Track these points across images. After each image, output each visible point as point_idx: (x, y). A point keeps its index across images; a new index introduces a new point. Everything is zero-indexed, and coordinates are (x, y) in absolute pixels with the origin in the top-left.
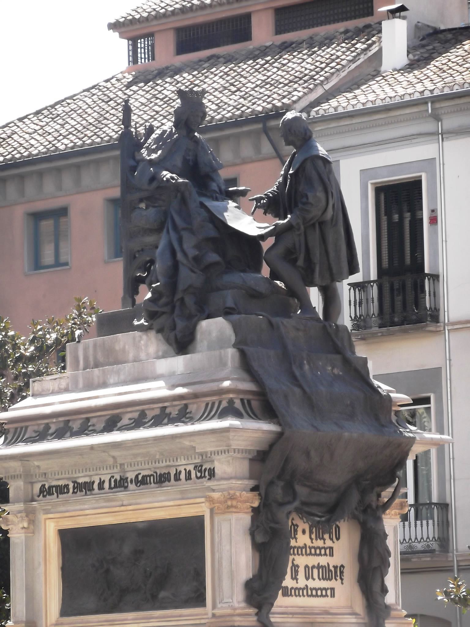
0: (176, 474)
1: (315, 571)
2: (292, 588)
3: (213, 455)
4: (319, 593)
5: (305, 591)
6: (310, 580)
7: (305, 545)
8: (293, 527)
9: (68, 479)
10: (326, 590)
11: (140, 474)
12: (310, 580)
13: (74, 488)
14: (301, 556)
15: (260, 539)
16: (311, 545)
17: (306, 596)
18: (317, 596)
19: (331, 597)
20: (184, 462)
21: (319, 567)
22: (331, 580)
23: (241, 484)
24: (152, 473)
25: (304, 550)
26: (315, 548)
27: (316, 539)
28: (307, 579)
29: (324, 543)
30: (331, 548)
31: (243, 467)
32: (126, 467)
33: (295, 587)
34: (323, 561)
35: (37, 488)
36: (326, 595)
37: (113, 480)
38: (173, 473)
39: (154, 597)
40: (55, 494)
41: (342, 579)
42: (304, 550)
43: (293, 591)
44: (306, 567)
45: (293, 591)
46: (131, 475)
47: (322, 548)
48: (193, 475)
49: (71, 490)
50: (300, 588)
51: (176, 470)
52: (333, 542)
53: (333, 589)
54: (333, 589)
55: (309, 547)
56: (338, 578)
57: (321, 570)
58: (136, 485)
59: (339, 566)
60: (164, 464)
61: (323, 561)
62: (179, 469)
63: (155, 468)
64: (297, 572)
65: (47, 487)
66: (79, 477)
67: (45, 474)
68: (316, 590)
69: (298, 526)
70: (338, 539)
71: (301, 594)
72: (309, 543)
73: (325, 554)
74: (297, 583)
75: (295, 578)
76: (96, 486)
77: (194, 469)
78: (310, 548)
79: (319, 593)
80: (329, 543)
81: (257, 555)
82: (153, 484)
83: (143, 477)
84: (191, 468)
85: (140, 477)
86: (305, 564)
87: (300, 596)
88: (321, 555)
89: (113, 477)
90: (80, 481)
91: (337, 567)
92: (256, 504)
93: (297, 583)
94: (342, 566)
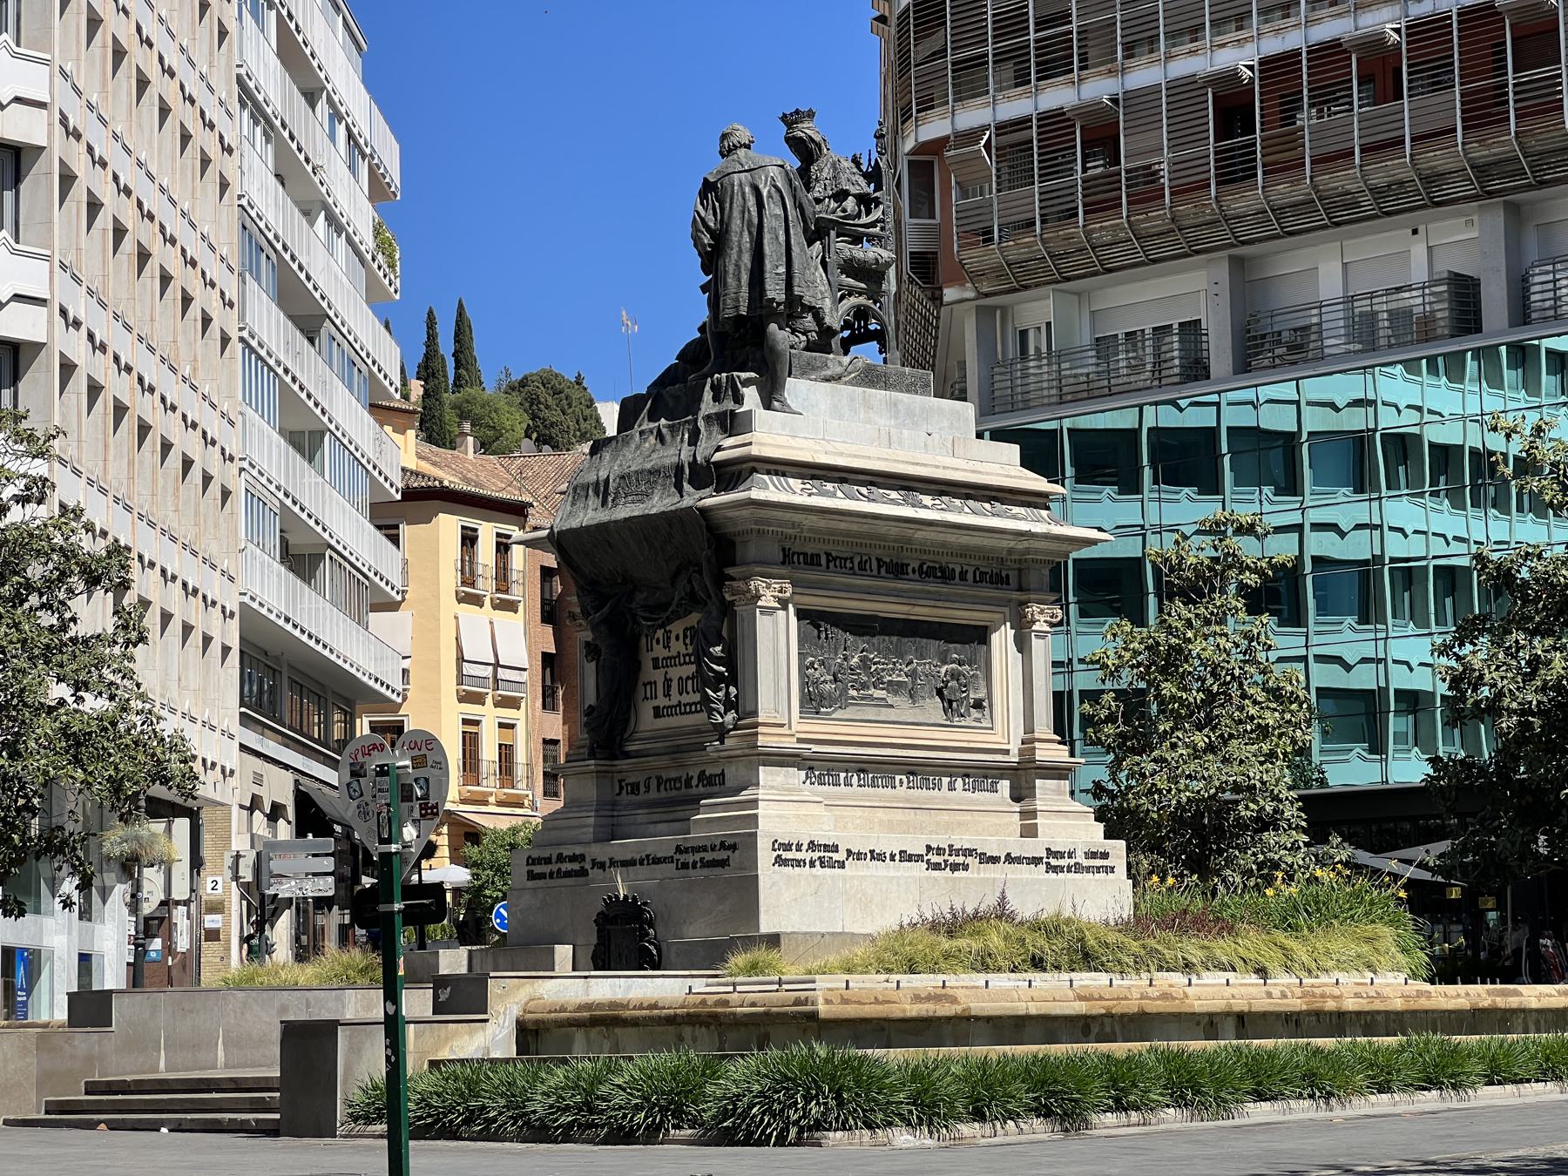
18: (691, 712)
28: (681, 694)
64: (669, 686)
68: (691, 705)
75: (667, 695)
78: (684, 656)
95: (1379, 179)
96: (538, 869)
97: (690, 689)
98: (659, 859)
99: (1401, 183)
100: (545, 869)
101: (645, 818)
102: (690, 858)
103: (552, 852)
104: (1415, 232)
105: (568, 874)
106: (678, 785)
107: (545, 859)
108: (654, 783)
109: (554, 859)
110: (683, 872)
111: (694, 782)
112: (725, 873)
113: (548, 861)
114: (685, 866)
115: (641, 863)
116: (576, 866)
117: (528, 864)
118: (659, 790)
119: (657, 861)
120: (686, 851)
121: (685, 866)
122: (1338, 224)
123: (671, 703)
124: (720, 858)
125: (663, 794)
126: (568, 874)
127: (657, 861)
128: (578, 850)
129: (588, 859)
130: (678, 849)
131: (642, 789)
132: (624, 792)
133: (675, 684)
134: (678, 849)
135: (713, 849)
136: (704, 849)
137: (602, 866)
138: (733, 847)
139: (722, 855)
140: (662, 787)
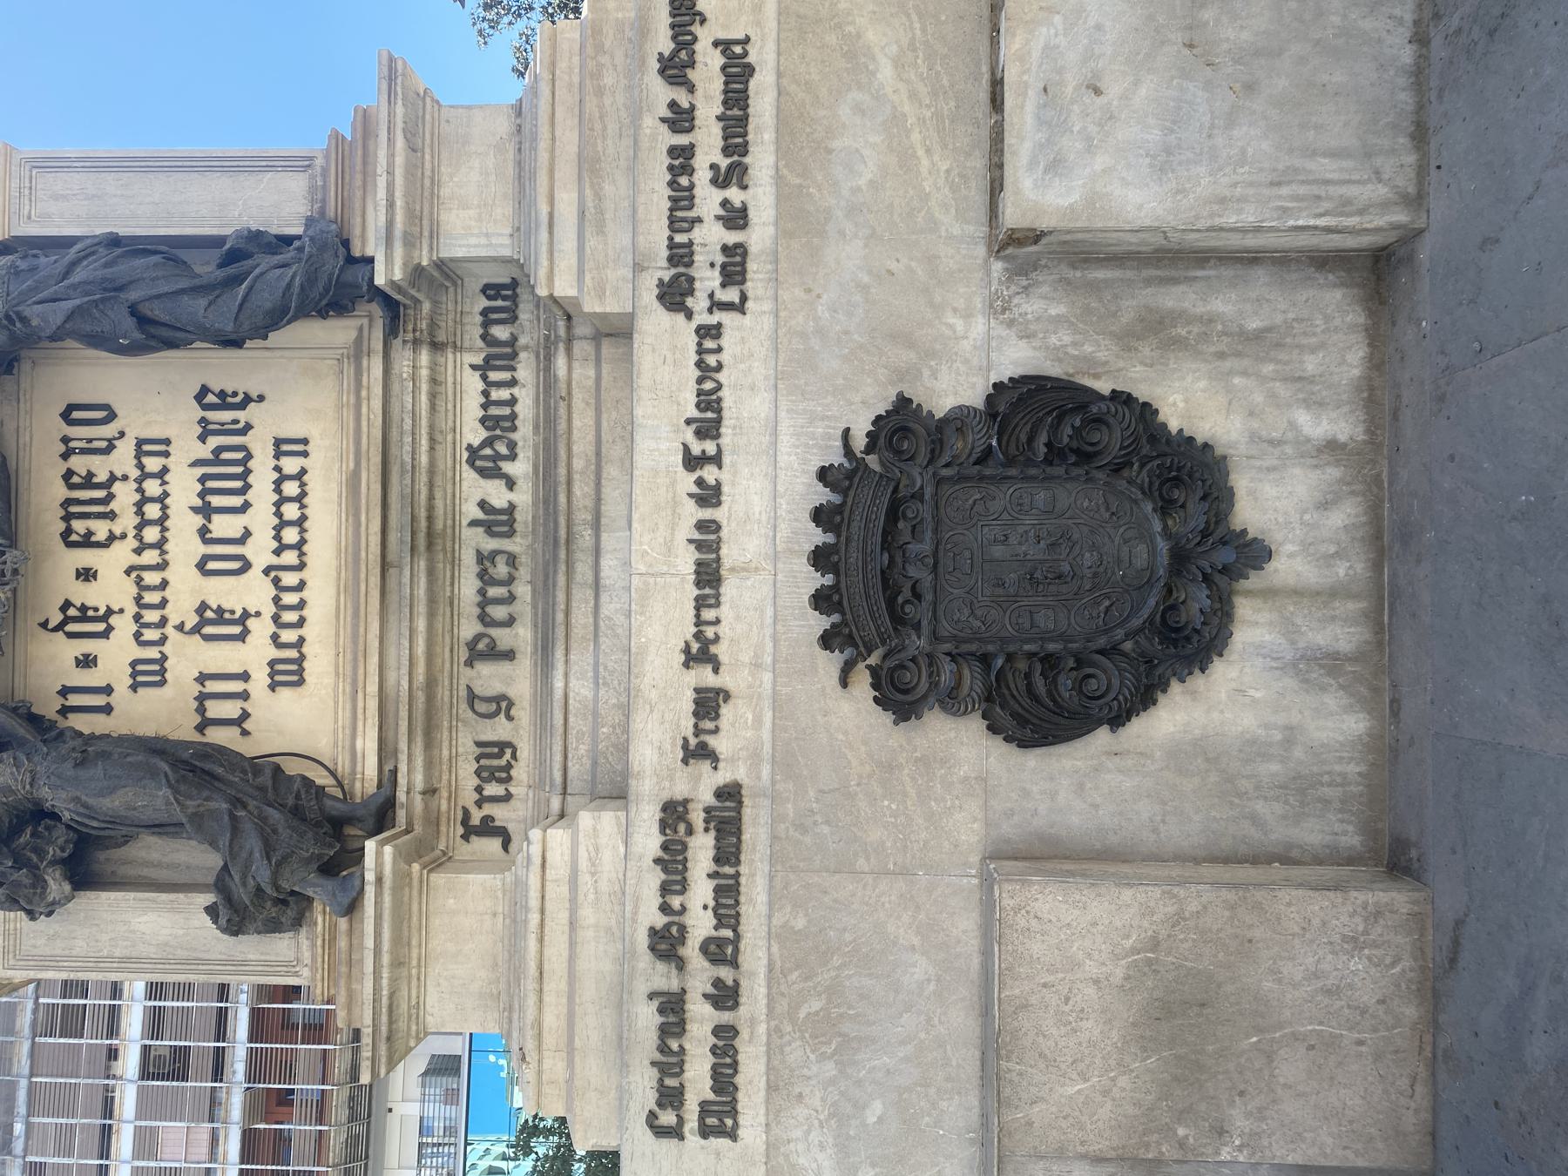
1: (224, 526)
5: (290, 579)
6: (247, 550)
8: (71, 628)
12: (247, 550)
14: (168, 593)
16: (131, 543)
17: (305, 574)
18: (300, 522)
19: (305, 454)
21: (206, 511)
22: (249, 456)
26: (144, 524)
28: (246, 566)
29: (125, 478)
33: (271, 628)
34: (183, 488)
36: (300, 475)
41: (247, 400)
47: (140, 490)
50: (276, 600)
52: (122, 434)
53: (280, 447)
54: (280, 447)
55: (138, 551)
56: (241, 415)
57: (216, 501)
64: (221, 616)
68: (283, 524)
69: (67, 604)
72: (122, 553)
74: (258, 614)
79: (291, 511)
80: (123, 459)
87: (302, 605)
88: (166, 494)
91: (203, 421)
93: (258, 614)
95: (344, 1114)
99: (351, 1098)
100: (702, 1017)
101: (582, 659)
102: (710, 236)
103: (642, 988)
104: (390, 1110)
105: (727, 894)
106: (501, 570)
107: (665, 1031)
108: (489, 678)
111: (498, 495)
112: (762, 56)
113: (672, 1007)
115: (709, 496)
116: (702, 849)
117: (676, 1133)
120: (681, 255)
121: (734, 267)
122: (367, 1157)
123: (269, 610)
124: (718, 84)
125: (522, 636)
126: (727, 894)
128: (649, 842)
129: (680, 790)
130: (675, 296)
131: (498, 730)
132: (500, 813)
134: (675, 296)
135: (681, 119)
136: (682, 159)
137: (708, 704)
139: (709, 68)
140: (503, 637)
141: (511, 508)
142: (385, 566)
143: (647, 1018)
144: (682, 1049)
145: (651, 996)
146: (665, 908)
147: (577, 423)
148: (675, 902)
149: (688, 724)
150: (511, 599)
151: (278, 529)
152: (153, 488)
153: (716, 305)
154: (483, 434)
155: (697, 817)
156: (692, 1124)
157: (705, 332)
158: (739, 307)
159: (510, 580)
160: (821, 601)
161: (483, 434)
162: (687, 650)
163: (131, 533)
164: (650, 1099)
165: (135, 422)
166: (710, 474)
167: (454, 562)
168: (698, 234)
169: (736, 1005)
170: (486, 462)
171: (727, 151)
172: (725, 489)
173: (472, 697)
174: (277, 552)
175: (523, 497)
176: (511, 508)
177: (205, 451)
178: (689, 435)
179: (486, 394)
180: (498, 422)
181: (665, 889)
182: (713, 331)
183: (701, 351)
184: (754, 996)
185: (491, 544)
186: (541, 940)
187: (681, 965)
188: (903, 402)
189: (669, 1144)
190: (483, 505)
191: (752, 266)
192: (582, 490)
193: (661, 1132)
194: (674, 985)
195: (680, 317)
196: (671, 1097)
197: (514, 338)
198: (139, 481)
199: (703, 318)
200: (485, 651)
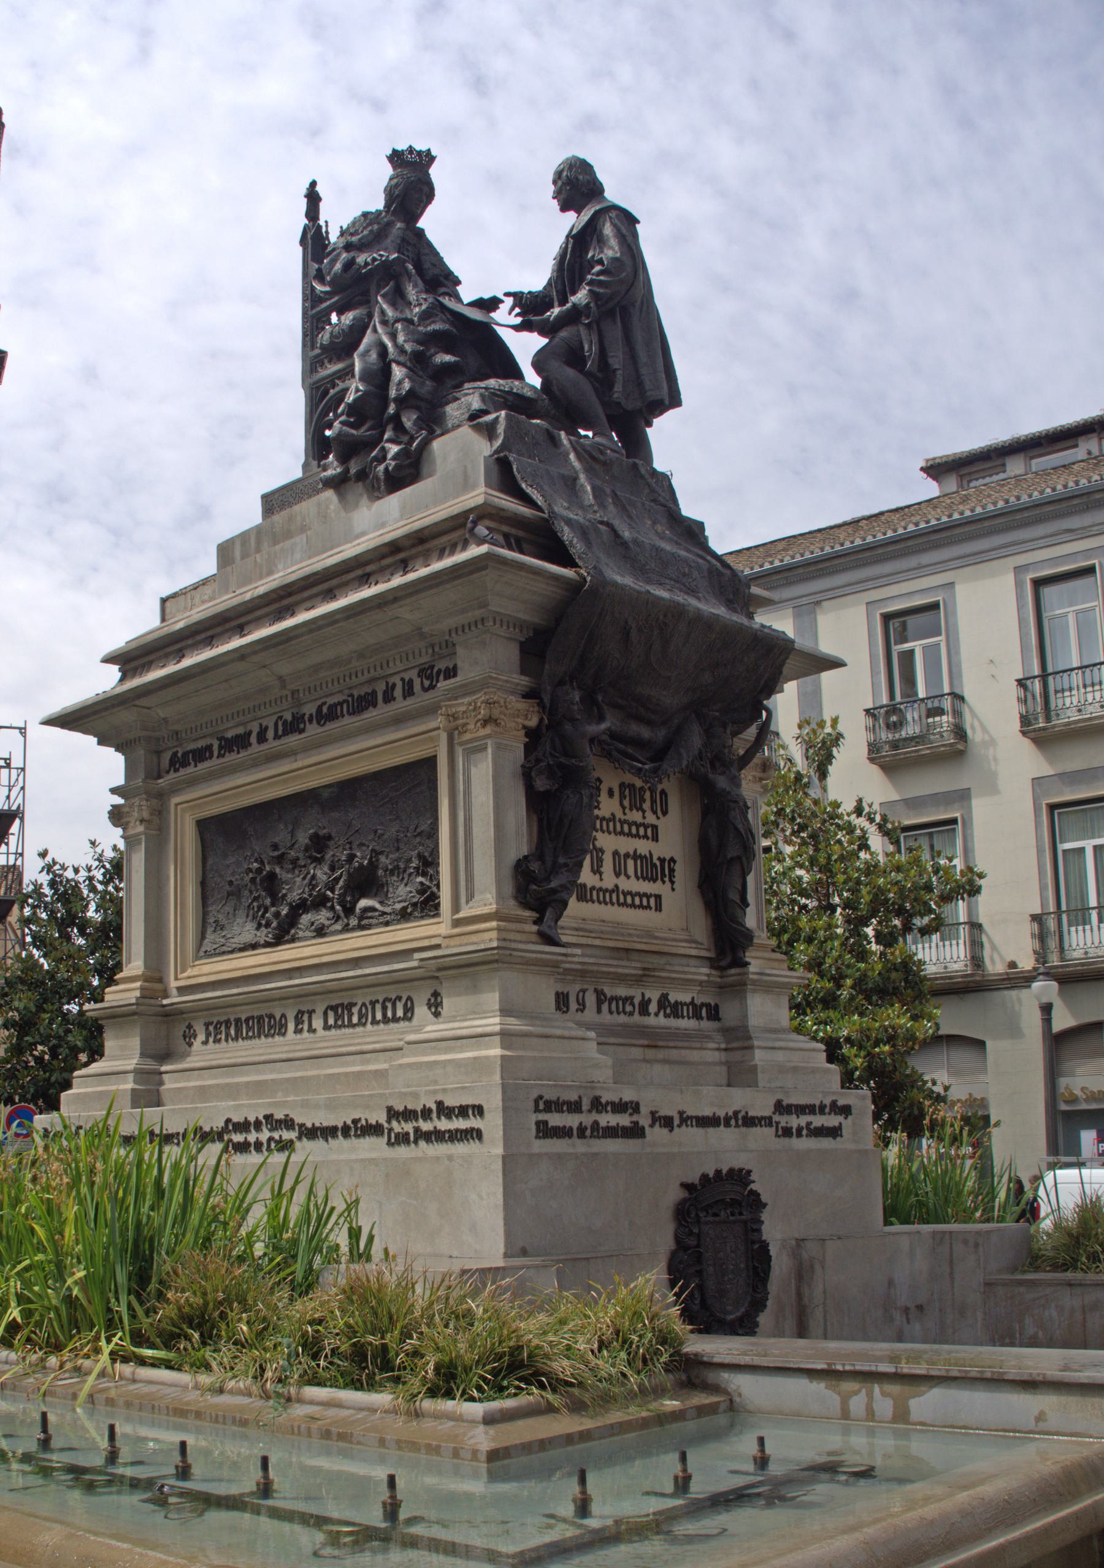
0: (385, 693)
1: (630, 863)
2: (593, 888)
3: (454, 635)
4: (637, 901)
6: (622, 877)
7: (613, 814)
9: (211, 735)
10: (648, 896)
11: (324, 703)
12: (622, 877)
13: (220, 747)
15: (541, 784)
16: (623, 817)
18: (633, 906)
20: (400, 666)
21: (636, 856)
22: (655, 881)
23: (507, 681)
24: (345, 697)
25: (611, 824)
26: (630, 824)
27: (631, 810)
29: (644, 818)
30: (655, 828)
31: (509, 654)
32: (301, 695)
34: (643, 847)
35: (167, 756)
36: (648, 907)
37: (280, 723)
38: (380, 687)
39: (349, 911)
40: (193, 764)
41: (672, 883)
42: (611, 824)
43: (595, 893)
44: (616, 853)
45: (595, 893)
46: (310, 709)
48: (417, 687)
49: (216, 753)
50: (607, 890)
51: (387, 683)
52: (658, 818)
53: (658, 897)
54: (658, 897)
55: (620, 820)
56: (667, 879)
58: (318, 723)
59: (668, 858)
60: (367, 676)
61: (643, 847)
62: (391, 681)
63: (350, 688)
64: (600, 861)
65: (179, 755)
66: (227, 729)
67: (177, 733)
70: (665, 813)
71: (608, 899)
73: (646, 837)
74: (601, 880)
75: (597, 870)
76: (253, 739)
77: (419, 676)
78: (622, 822)
80: (651, 819)
81: (535, 818)
82: (346, 716)
83: (330, 707)
84: (413, 674)
85: (325, 709)
86: (613, 848)
89: (281, 718)
90: (229, 735)
91: (664, 859)
92: (533, 722)
93: (601, 880)
94: (672, 860)
96: (555, 1120)
97: (631, 871)
98: (753, 1118)
100: (571, 1120)
102: (794, 1121)
105: (612, 1132)
106: (628, 1008)
108: (591, 999)
109: (586, 1104)
110: (785, 1141)
111: (653, 1007)
114: (787, 1132)
116: (624, 1120)
117: (537, 1110)
118: (599, 1011)
119: (750, 1122)
121: (787, 1132)
126: (612, 1132)
127: (750, 1122)
129: (644, 1110)
130: (781, 1108)
131: (573, 1006)
133: (608, 859)
134: (781, 1108)
135: (822, 1109)
138: (846, 1111)
139: (832, 1121)
140: (605, 1007)
141: (649, 1015)
142: (627, 950)
143: (573, 1097)
144: (563, 1112)
145: (580, 1097)
146: (607, 1103)
147: (695, 1052)
148: (609, 1108)
149: (662, 1113)
150: (619, 1013)
151: (630, 893)
152: (642, 831)
153: (777, 1123)
154: (672, 1001)
155: (635, 1118)
156: (542, 1117)
157: (770, 1118)
158: (777, 1136)
159: (625, 1013)
160: (718, 1172)
161: (672, 1001)
162: (684, 1112)
163: (626, 817)
164: (547, 1097)
165: (663, 824)
166: (733, 1122)
167: (631, 986)
168: (794, 1116)
169: (579, 1137)
170: (663, 1002)
171: (816, 1128)
172: (729, 1129)
173: (584, 991)
174: (623, 892)
175: (651, 1020)
176: (649, 1015)
177: (655, 860)
178: (743, 1113)
179: (685, 1004)
180: (675, 1010)
181: (613, 1104)
182: (770, 1125)
183: (763, 1118)
184: (579, 1146)
185: (637, 1001)
186: (559, 1037)
187: (590, 1111)
188: (765, 1205)
189: (532, 1104)
190: (650, 1000)
191: (787, 1139)
192: (674, 1054)
193: (536, 1102)
194: (585, 1108)
195: (773, 1109)
196: (551, 1106)
197: (702, 1018)
198: (643, 825)
199: (776, 1118)
200: (601, 998)
